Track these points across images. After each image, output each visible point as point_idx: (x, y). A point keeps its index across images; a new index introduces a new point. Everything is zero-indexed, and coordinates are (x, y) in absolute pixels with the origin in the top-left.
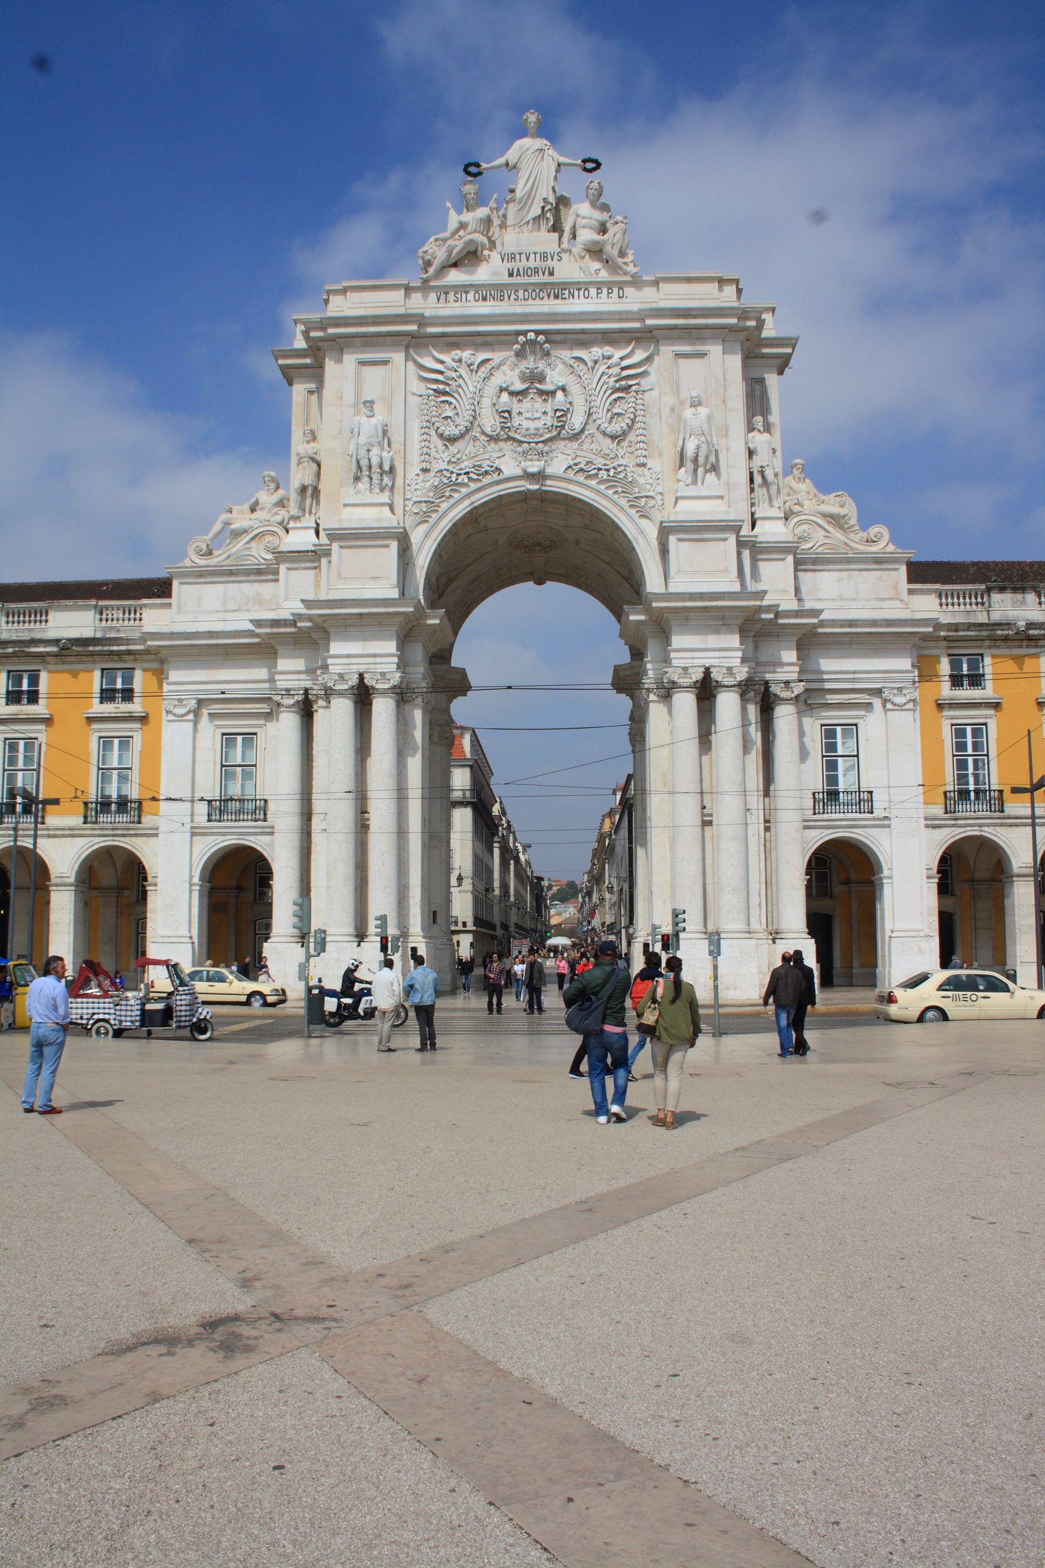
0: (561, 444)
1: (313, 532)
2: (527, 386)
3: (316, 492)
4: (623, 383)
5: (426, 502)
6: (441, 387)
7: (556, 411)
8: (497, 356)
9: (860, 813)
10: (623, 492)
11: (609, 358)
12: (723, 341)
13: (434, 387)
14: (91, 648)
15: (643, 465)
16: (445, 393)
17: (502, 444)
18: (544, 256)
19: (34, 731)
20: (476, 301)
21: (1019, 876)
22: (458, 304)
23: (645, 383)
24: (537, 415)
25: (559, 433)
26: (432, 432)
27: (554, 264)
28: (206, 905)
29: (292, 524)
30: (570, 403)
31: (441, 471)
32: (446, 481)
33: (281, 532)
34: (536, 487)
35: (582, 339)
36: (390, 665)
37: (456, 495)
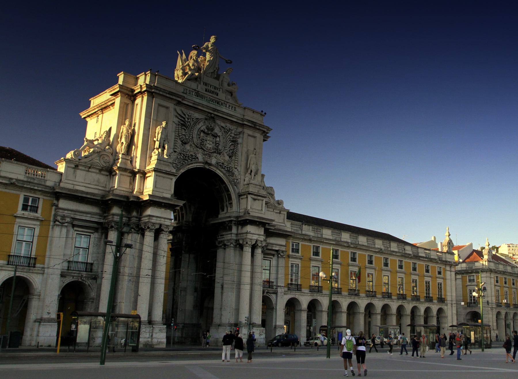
0: (215, 155)
2: (210, 132)
5: (175, 163)
9: (269, 288)
10: (231, 176)
11: (232, 130)
12: (260, 134)
13: (182, 123)
14: (25, 186)
15: (236, 168)
17: (198, 149)
18: (215, 88)
20: (195, 96)
21: (303, 310)
22: (190, 95)
26: (178, 138)
27: (218, 91)
31: (181, 154)
33: (110, 155)
37: (184, 163)
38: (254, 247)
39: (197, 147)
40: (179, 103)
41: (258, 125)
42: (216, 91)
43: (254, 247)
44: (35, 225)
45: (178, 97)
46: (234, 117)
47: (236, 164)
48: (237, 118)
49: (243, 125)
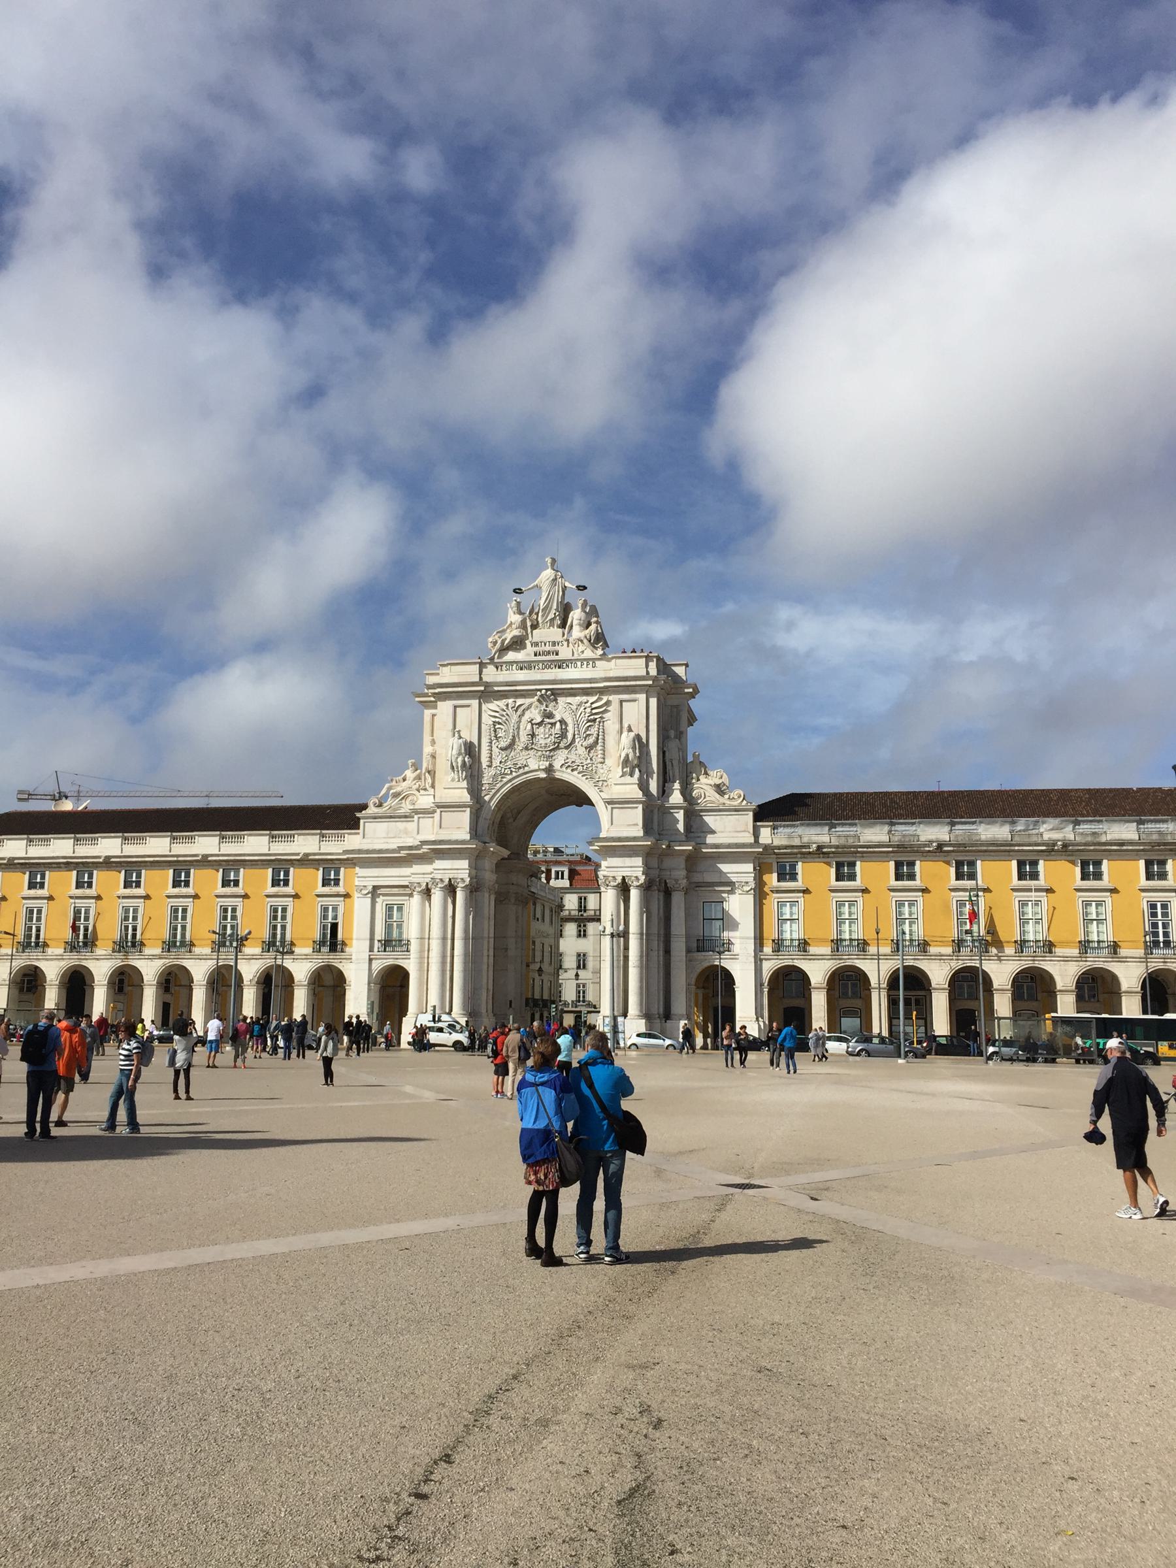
1: (432, 797)
3: (435, 772)
4: (592, 717)
6: (497, 720)
8: (528, 701)
15: (601, 763)
16: (499, 723)
18: (554, 644)
19: (286, 902)
21: (814, 988)
28: (376, 998)
29: (422, 792)
33: (416, 793)
34: (545, 776)
35: (572, 693)
36: (465, 875)
42: (557, 648)
43: (624, 889)
44: (339, 901)
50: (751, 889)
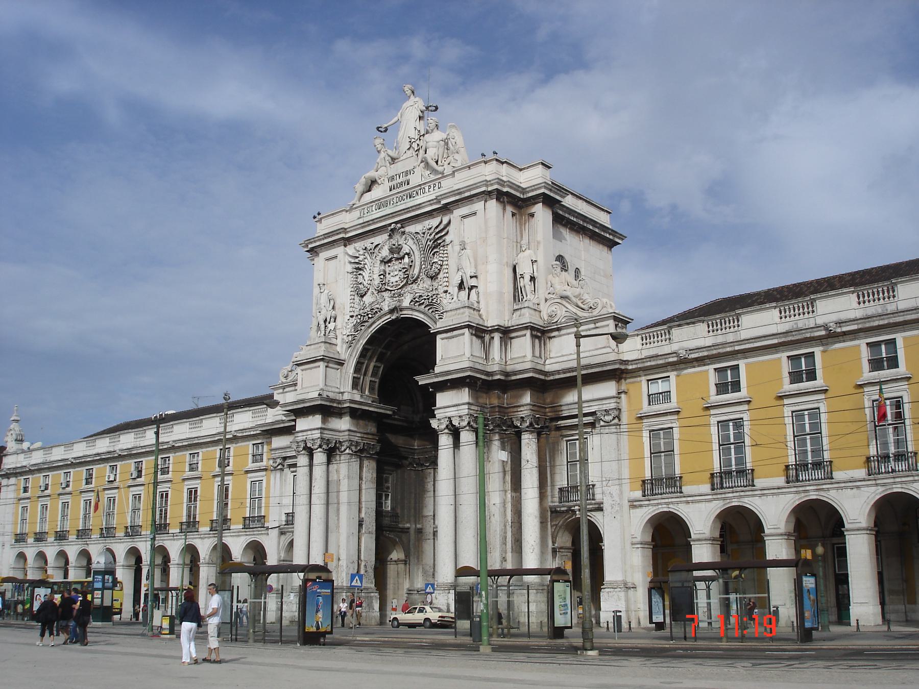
0: (409, 288)
7: (403, 268)
14: (244, 434)
15: (446, 292)
16: (360, 269)
17: (384, 294)
18: (407, 173)
21: (694, 541)
23: (448, 239)
24: (396, 273)
25: (407, 282)
30: (412, 261)
32: (359, 321)
37: (363, 328)
38: (455, 433)
39: (382, 291)
40: (347, 241)
41: (464, 189)
43: (455, 433)
45: (338, 234)
46: (423, 205)
47: (445, 284)
48: (429, 203)
49: (446, 209)
50: (614, 418)
